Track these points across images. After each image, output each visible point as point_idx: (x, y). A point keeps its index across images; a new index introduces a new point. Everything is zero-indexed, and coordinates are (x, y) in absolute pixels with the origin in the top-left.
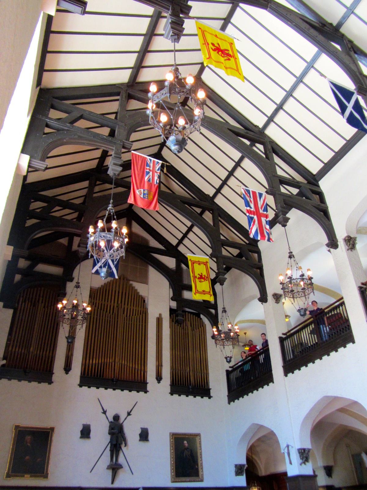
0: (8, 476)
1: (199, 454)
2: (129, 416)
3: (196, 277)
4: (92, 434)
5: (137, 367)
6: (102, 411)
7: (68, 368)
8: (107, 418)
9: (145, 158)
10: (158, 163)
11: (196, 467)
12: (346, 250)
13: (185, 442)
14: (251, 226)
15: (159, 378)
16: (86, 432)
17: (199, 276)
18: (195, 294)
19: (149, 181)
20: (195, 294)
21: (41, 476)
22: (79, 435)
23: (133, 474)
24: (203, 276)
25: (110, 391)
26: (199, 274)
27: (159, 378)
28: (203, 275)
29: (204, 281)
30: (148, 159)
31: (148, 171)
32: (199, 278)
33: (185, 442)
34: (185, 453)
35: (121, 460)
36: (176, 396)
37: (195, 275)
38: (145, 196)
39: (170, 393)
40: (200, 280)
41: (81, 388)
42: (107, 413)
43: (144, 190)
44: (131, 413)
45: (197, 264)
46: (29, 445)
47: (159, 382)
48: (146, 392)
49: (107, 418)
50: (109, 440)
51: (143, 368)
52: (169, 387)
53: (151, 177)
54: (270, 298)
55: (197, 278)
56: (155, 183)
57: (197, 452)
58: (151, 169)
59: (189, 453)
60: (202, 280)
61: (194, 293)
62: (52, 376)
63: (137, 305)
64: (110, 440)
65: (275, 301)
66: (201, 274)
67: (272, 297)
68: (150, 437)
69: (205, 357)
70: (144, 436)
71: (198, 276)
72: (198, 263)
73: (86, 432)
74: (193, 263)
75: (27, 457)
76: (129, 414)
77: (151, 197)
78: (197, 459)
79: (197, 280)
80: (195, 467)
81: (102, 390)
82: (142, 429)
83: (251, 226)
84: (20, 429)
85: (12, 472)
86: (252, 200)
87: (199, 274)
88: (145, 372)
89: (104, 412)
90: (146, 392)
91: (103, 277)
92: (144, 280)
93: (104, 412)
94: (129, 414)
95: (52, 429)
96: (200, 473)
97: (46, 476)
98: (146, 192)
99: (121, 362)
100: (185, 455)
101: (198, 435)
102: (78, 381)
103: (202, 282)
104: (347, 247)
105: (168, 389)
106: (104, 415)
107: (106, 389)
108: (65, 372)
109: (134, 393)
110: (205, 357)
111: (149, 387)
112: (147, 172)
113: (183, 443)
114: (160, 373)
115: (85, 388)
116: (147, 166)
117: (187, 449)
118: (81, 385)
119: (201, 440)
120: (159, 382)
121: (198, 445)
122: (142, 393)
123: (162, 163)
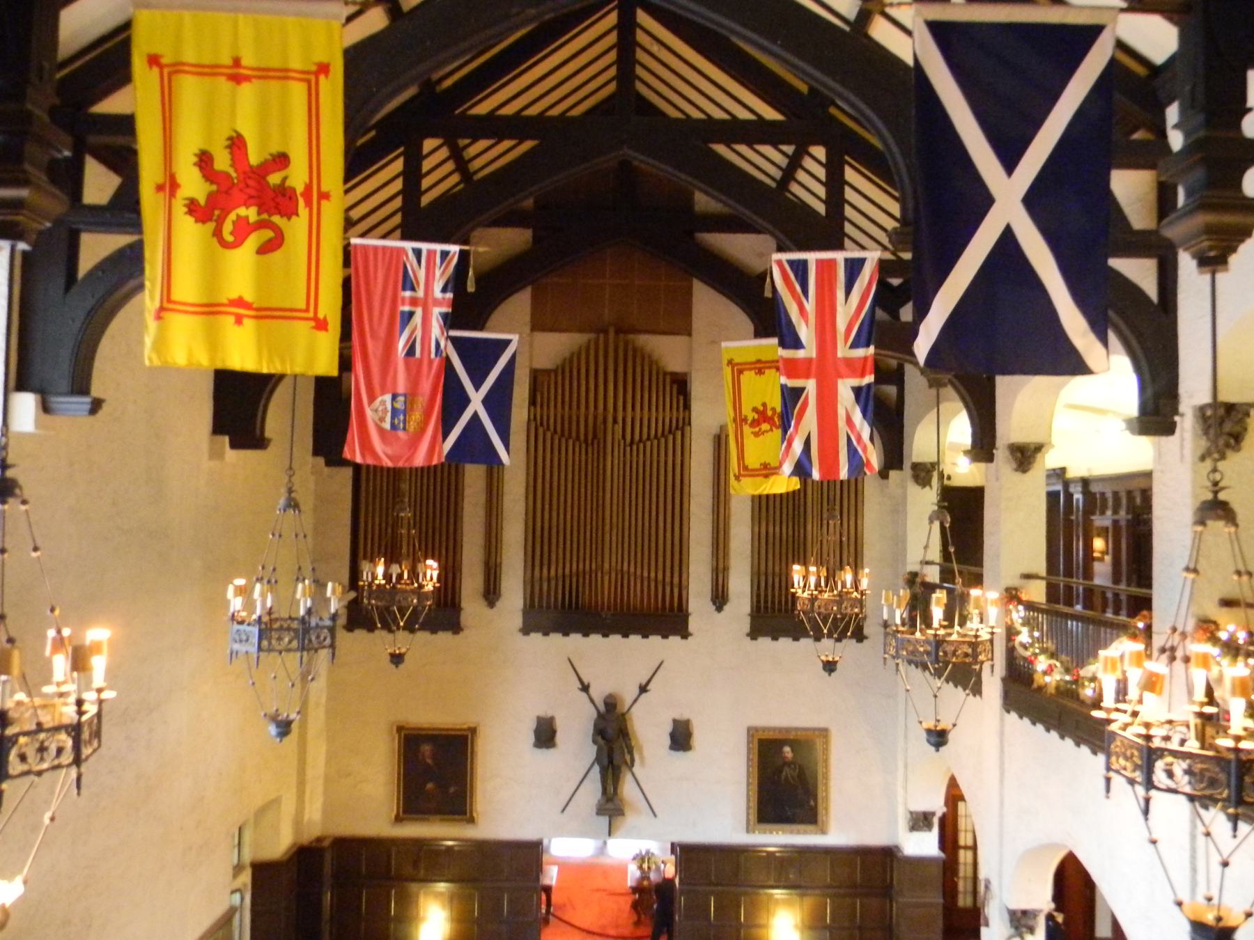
0: (398, 819)
1: (820, 777)
2: (644, 695)
3: (745, 420)
4: (559, 738)
5: (660, 577)
6: (580, 686)
7: (491, 593)
8: (592, 701)
9: (401, 251)
10: (445, 254)
11: (812, 803)
12: (1196, 460)
13: (787, 749)
14: (790, 427)
15: (720, 598)
16: (545, 735)
17: (756, 416)
18: (737, 478)
19: (411, 352)
20: (737, 478)
21: (462, 820)
22: (531, 738)
23: (655, 816)
24: (770, 413)
25: (596, 639)
26: (755, 410)
27: (720, 598)
28: (769, 407)
29: (771, 430)
30: (410, 253)
31: (407, 308)
32: (755, 423)
33: (787, 749)
34: (784, 773)
35: (628, 788)
36: (765, 642)
37: (744, 412)
38: (396, 421)
39: (748, 635)
40: (757, 429)
41: (526, 638)
42: (592, 690)
43: (394, 398)
44: (648, 688)
45: (753, 372)
46: (429, 761)
47: (719, 609)
48: (685, 635)
49: (592, 701)
50: (594, 756)
51: (676, 580)
52: (748, 620)
53: (419, 334)
54: (1001, 453)
55: (749, 422)
56: (433, 355)
57: (817, 771)
58: (420, 293)
59: (795, 774)
60: (765, 426)
61: (735, 475)
62: (458, 617)
63: (546, 562)
64: (597, 754)
65: (1014, 465)
66: (761, 408)
67: (1007, 453)
68: (697, 739)
69: (856, 533)
70: (681, 738)
71: (751, 416)
72: (755, 368)
73: (545, 735)
74: (741, 372)
75: (430, 786)
76: (643, 689)
77: (417, 416)
78: (816, 787)
79: (747, 430)
80: (808, 802)
81: (576, 638)
82: (675, 721)
83: (792, 429)
84: (407, 732)
85: (405, 812)
86: (810, 306)
87: (755, 410)
88: (682, 587)
89: (585, 688)
90: (685, 635)
91: (386, 583)
92: (681, 324)
93: (585, 688)
94: (643, 689)
95: (473, 731)
96: (820, 818)
97: (471, 820)
98: (400, 404)
99: (619, 568)
100: (783, 777)
101: (824, 733)
102: (518, 621)
103: (763, 433)
104: (1204, 443)
105: (746, 625)
106: (584, 695)
107: (586, 635)
108: (485, 603)
109: (655, 640)
110: (856, 533)
111: (693, 624)
112: (403, 313)
113: (780, 751)
114: (723, 591)
115: (536, 637)
116: (404, 289)
117: (787, 764)
118: (526, 630)
119: (827, 746)
120: (719, 609)
121: (820, 756)
122: (675, 640)
123: (461, 252)
